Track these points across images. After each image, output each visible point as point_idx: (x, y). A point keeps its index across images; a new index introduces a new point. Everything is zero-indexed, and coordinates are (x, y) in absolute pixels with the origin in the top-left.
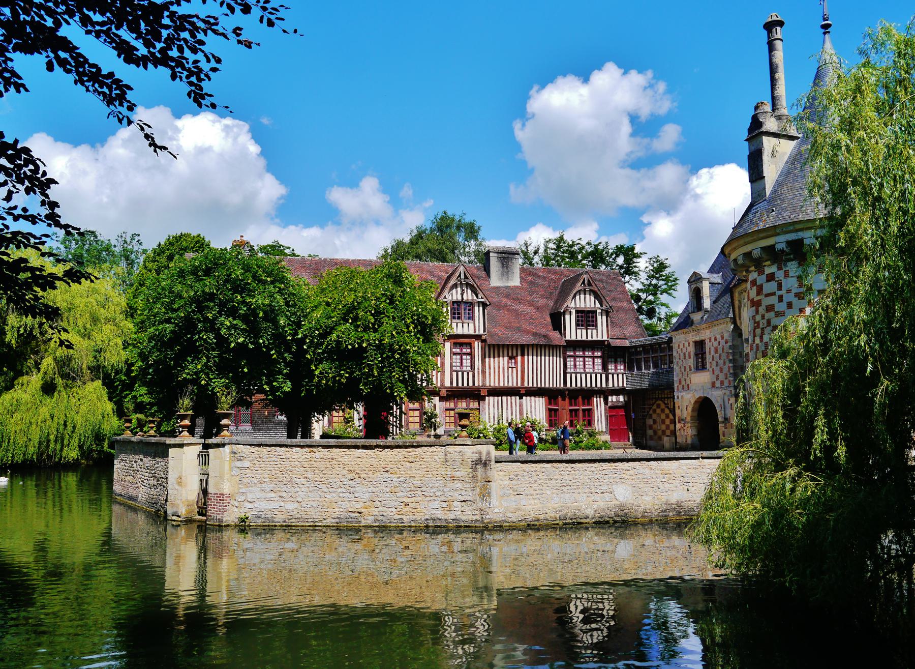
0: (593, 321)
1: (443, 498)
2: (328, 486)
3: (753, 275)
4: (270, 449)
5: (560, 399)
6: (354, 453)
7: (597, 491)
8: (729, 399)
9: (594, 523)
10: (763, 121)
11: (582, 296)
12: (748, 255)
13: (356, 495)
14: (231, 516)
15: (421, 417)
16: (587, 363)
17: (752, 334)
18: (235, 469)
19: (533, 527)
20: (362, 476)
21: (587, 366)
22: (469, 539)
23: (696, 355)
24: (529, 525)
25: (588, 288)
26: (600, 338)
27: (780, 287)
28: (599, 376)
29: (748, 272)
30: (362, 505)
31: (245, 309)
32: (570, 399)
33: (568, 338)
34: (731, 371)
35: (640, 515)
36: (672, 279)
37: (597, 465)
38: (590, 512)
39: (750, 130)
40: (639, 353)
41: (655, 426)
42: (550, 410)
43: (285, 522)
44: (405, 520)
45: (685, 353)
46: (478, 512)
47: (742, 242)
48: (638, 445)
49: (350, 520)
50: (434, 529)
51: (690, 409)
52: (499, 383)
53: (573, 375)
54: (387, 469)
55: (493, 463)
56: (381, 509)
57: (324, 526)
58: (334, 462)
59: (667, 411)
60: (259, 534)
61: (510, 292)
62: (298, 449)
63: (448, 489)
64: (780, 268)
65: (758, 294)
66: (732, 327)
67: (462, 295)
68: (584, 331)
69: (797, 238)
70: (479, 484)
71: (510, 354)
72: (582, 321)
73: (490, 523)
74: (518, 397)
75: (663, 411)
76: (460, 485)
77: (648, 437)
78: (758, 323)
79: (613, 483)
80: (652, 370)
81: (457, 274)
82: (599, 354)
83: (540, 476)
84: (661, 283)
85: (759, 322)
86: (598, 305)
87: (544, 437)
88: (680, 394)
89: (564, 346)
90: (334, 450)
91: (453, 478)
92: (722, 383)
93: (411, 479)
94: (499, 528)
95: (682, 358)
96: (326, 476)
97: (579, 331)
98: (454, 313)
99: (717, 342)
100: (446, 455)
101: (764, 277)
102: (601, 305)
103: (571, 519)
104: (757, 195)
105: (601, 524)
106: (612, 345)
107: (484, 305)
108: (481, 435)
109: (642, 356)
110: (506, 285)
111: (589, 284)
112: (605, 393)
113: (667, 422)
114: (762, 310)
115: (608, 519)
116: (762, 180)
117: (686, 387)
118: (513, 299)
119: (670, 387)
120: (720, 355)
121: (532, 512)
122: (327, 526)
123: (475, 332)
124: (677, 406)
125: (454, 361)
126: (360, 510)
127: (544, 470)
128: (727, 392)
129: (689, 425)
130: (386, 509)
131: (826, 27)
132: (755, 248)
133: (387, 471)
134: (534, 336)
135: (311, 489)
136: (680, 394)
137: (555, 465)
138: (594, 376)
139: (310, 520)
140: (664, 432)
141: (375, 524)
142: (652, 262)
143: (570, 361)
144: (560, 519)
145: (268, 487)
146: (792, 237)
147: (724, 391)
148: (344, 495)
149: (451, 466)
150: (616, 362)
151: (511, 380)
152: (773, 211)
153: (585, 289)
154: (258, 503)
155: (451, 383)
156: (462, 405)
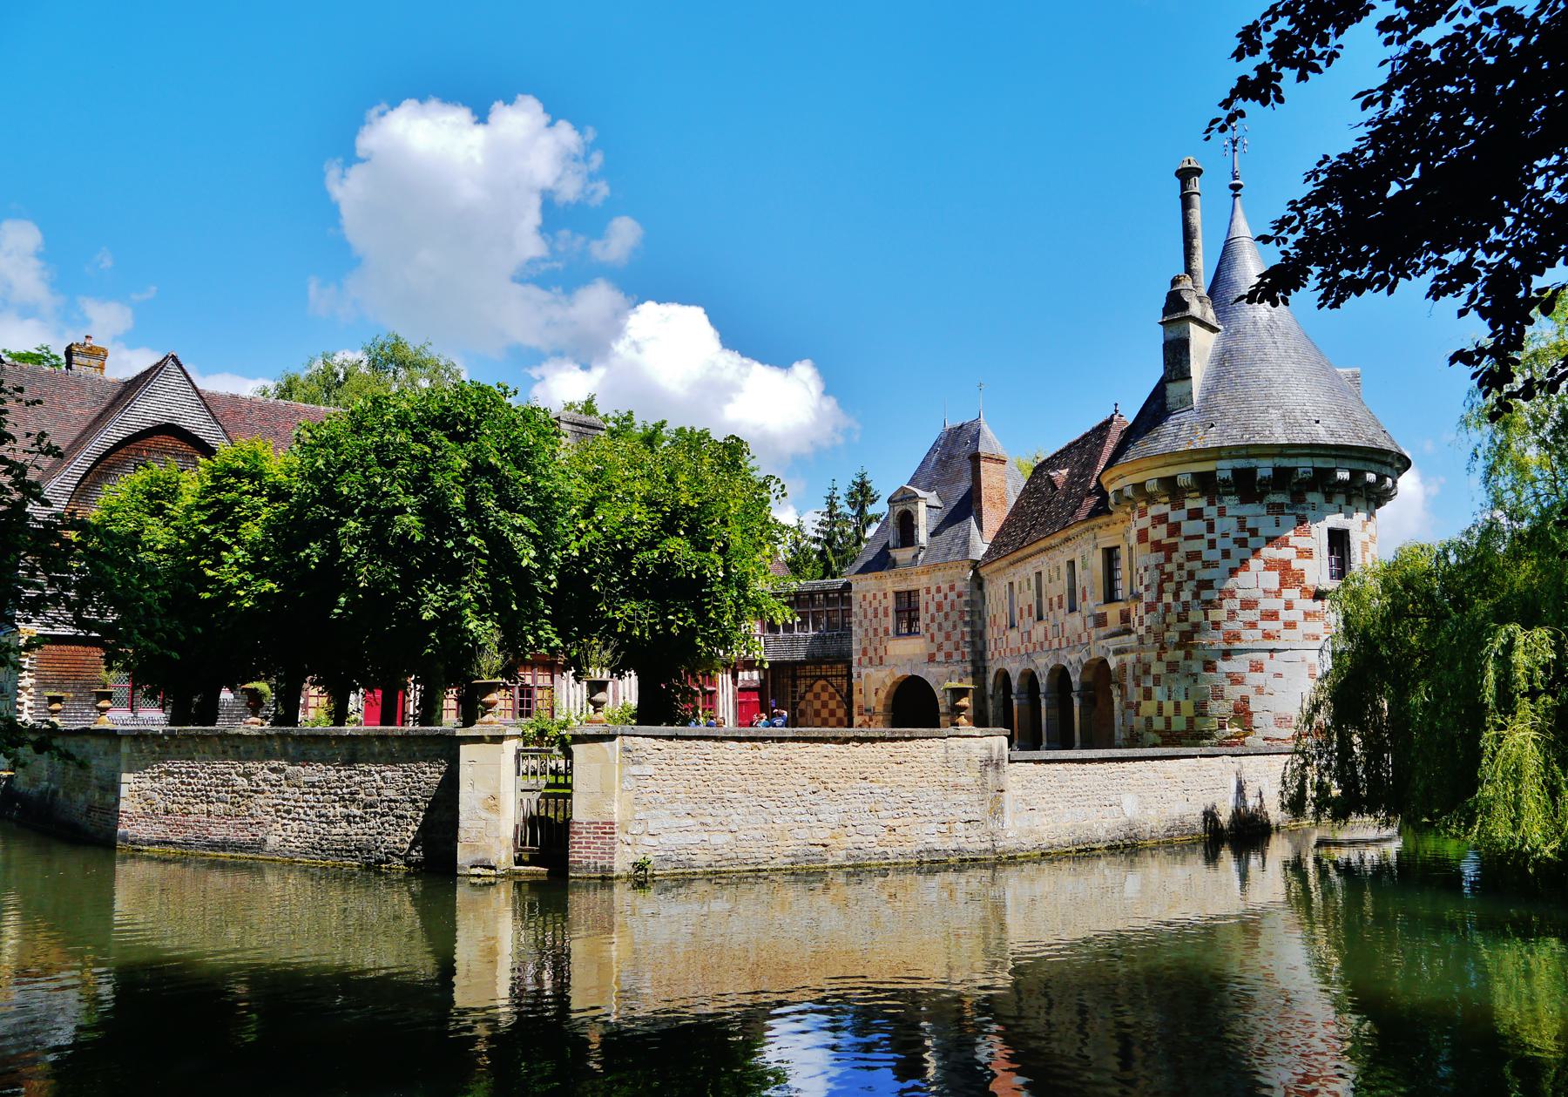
1: (941, 819)
2: (779, 804)
6: (819, 749)
7: (1107, 803)
10: (1190, 301)
14: (622, 864)
17: (1154, 589)
18: (628, 778)
19: (1047, 856)
20: (830, 786)
22: (973, 880)
23: (897, 611)
24: (1043, 854)
27: (1211, 527)
31: (531, 497)
34: (968, 639)
35: (1148, 836)
37: (1106, 765)
38: (1101, 834)
39: (1166, 311)
43: (710, 866)
44: (891, 855)
45: (876, 609)
46: (988, 838)
47: (1162, 462)
49: (811, 858)
50: (930, 865)
51: (882, 695)
54: (866, 775)
56: (856, 838)
57: (772, 870)
58: (789, 764)
60: (667, 889)
62: (735, 743)
64: (1211, 503)
65: (1171, 534)
66: (971, 573)
69: (1248, 466)
76: (964, 797)
78: (1170, 576)
79: (1121, 791)
80: (811, 633)
85: (1172, 573)
88: (864, 672)
91: (955, 786)
92: (949, 655)
94: (1012, 860)
96: (776, 787)
99: (942, 595)
100: (947, 752)
105: (1113, 849)
117: (876, 660)
119: (845, 659)
120: (947, 615)
121: (1045, 836)
122: (778, 870)
124: (855, 689)
126: (826, 842)
127: (1056, 773)
128: (958, 669)
129: (881, 718)
130: (863, 838)
131: (1236, 187)
133: (865, 779)
135: (752, 809)
136: (864, 672)
139: (750, 861)
141: (848, 863)
145: (682, 809)
146: (1240, 464)
147: (951, 668)
148: (803, 818)
152: (1212, 426)
154: (665, 835)
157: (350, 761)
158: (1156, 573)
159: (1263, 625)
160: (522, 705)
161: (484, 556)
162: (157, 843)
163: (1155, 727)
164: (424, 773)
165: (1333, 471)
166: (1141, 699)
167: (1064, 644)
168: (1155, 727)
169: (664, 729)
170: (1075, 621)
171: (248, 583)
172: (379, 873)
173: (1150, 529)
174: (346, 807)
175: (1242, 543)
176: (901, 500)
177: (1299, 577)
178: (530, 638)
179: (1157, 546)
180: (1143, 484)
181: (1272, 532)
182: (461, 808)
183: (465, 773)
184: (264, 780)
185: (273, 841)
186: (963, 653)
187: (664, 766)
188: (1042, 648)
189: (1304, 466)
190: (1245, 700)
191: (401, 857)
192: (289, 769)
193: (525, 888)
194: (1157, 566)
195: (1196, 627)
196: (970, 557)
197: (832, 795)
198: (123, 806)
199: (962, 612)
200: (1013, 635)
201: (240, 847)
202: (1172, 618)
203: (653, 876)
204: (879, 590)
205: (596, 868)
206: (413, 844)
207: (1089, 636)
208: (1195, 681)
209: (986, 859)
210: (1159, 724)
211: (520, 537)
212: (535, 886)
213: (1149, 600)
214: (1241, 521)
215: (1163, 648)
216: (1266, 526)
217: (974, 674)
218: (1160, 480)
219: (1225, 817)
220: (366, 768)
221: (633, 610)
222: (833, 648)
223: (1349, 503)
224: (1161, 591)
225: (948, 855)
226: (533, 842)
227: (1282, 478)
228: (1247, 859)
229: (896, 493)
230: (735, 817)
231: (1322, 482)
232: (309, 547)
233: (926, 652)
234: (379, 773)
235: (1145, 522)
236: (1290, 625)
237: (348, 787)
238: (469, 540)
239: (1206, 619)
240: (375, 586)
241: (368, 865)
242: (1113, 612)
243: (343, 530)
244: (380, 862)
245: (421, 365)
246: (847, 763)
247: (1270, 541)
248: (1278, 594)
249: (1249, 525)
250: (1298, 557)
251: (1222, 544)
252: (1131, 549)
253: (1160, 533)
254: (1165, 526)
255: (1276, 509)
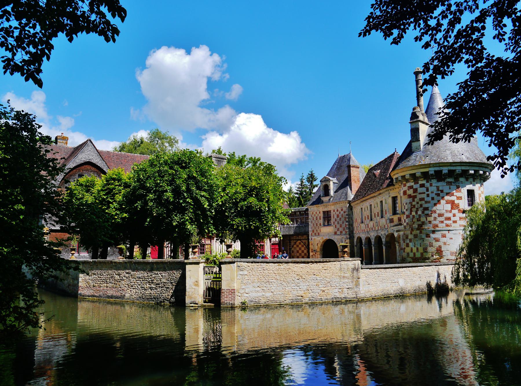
1: (340, 287)
4: (258, 264)
8: (345, 240)
13: (300, 287)
14: (237, 302)
17: (409, 210)
18: (239, 275)
19: (374, 299)
20: (303, 277)
22: (350, 306)
23: (324, 218)
24: (373, 299)
27: (427, 190)
30: (303, 292)
37: (393, 269)
38: (392, 292)
39: (411, 119)
43: (265, 303)
45: (317, 217)
47: (411, 169)
50: (336, 302)
51: (319, 245)
56: (312, 294)
57: (285, 304)
60: (252, 310)
64: (427, 182)
65: (414, 193)
66: (348, 205)
70: (355, 280)
78: (414, 206)
80: (295, 225)
83: (375, 275)
88: (313, 238)
90: (290, 264)
91: (344, 277)
92: (341, 232)
93: (326, 278)
96: (286, 278)
99: (339, 212)
101: (418, 185)
105: (396, 297)
113: (300, 252)
114: (416, 200)
119: (307, 234)
120: (340, 219)
124: (310, 244)
126: (302, 295)
128: (345, 237)
129: (319, 253)
135: (278, 285)
136: (313, 238)
139: (278, 302)
145: (256, 285)
147: (342, 236)
148: (295, 287)
157: (151, 270)
158: (410, 205)
159: (446, 222)
160: (201, 250)
161: (192, 205)
162: (91, 296)
163: (410, 256)
164: (175, 274)
165: (468, 171)
166: (405, 247)
167: (380, 228)
168: (410, 256)
169: (249, 259)
170: (383, 221)
171: (118, 214)
172: (161, 306)
173: (407, 191)
174: (150, 285)
175: (438, 195)
176: (325, 181)
177: (457, 206)
178: (206, 230)
179: (410, 196)
180: (405, 176)
181: (448, 191)
182: (187, 285)
183: (188, 274)
184: (124, 276)
185: (127, 295)
186: (346, 231)
187: (250, 271)
188: (372, 229)
189: (459, 169)
190: (440, 247)
191: (168, 301)
192: (132, 273)
193: (207, 310)
194: (410, 203)
195: (423, 223)
196: (348, 199)
197: (304, 280)
198: (80, 284)
199: (345, 218)
200: (363, 225)
201: (117, 297)
202: (415, 220)
203: (247, 306)
205: (229, 304)
206: (172, 296)
207: (388, 226)
208: (423, 241)
210: (411, 255)
211: (203, 198)
212: (210, 309)
213: (407, 214)
214: (438, 188)
215: (412, 230)
216: (446, 189)
217: (350, 238)
218: (410, 174)
219: (433, 286)
220: (156, 272)
221: (239, 221)
222: (302, 230)
223: (474, 181)
224: (411, 211)
226: (209, 296)
227: (451, 173)
228: (442, 300)
229: (323, 179)
230: (273, 287)
231: (465, 174)
232: (137, 203)
233: (333, 231)
234: (160, 274)
235: (406, 188)
236: (455, 222)
237: (151, 278)
238: (187, 200)
239: (427, 220)
240: (159, 215)
241: (157, 303)
242: (396, 218)
243: (148, 197)
244: (161, 302)
245: (166, 139)
246: (309, 271)
247: (447, 194)
248: (451, 212)
249: (440, 189)
250: (457, 199)
251: (431, 195)
252: (401, 197)
253: (410, 192)
254: (412, 189)
255: (450, 183)
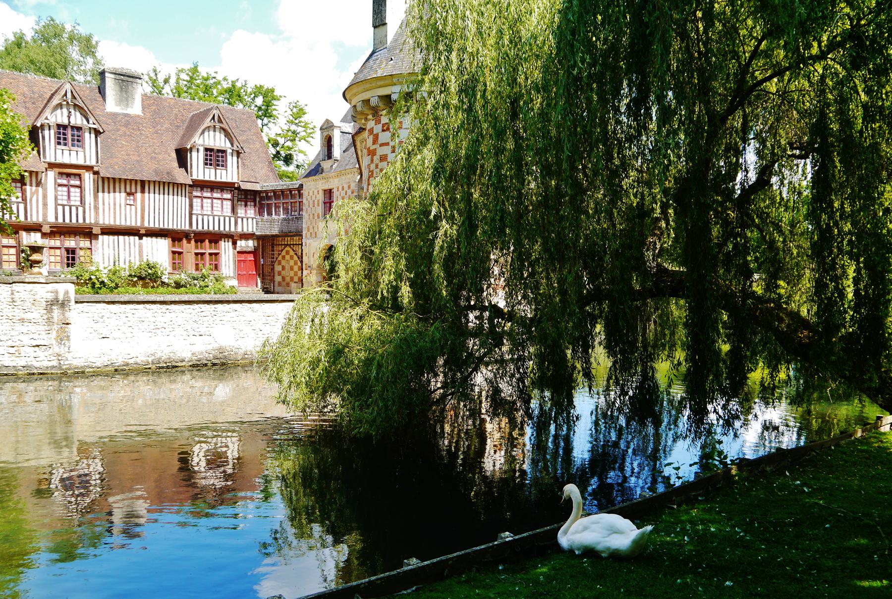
0: (223, 161)
1: (10, 343)
3: (371, 124)
5: (185, 241)
9: (191, 366)
11: (212, 133)
12: (366, 102)
15: (18, 255)
16: (214, 205)
21: (214, 209)
24: (116, 370)
25: (218, 125)
26: (229, 180)
28: (227, 219)
29: (366, 119)
32: (196, 242)
33: (195, 177)
35: (240, 357)
36: (311, 127)
37: (196, 306)
40: (269, 198)
41: (283, 273)
42: (174, 253)
45: (314, 201)
48: (266, 291)
51: (317, 256)
52: (115, 221)
53: (200, 218)
55: (73, 303)
59: (296, 258)
61: (129, 121)
63: (17, 333)
65: (374, 143)
67: (69, 117)
68: (213, 171)
70: (55, 327)
71: (128, 190)
72: (211, 160)
73: (69, 369)
74: (137, 238)
75: (292, 257)
76: (32, 328)
77: (276, 283)
80: (282, 216)
81: (63, 93)
82: (229, 196)
84: (300, 129)
86: (228, 145)
87: (166, 281)
88: (308, 242)
89: (190, 186)
91: (22, 320)
94: (80, 374)
95: (311, 205)
97: (207, 170)
98: (59, 138)
99: (344, 192)
100: (12, 294)
102: (232, 145)
103: (166, 363)
104: (379, 44)
105: (198, 367)
106: (243, 187)
107: (97, 133)
108: (93, 277)
109: (273, 201)
110: (125, 112)
111: (220, 121)
112: (233, 238)
113: (296, 268)
115: (206, 362)
116: (385, 26)
117: (314, 235)
118: (133, 129)
119: (299, 234)
123: (85, 162)
125: (59, 193)
127: (134, 311)
132: (374, 96)
134: (156, 172)
136: (308, 242)
137: (147, 306)
138: (222, 219)
140: (292, 279)
142: (291, 107)
143: (197, 202)
144: (153, 363)
149: (20, 307)
150: (246, 205)
151: (130, 220)
153: (214, 126)
155: (56, 218)
156: (71, 243)
160: (68, 259)
204: (316, 189)
209: (52, 374)
222: (293, 227)
225: (16, 370)
